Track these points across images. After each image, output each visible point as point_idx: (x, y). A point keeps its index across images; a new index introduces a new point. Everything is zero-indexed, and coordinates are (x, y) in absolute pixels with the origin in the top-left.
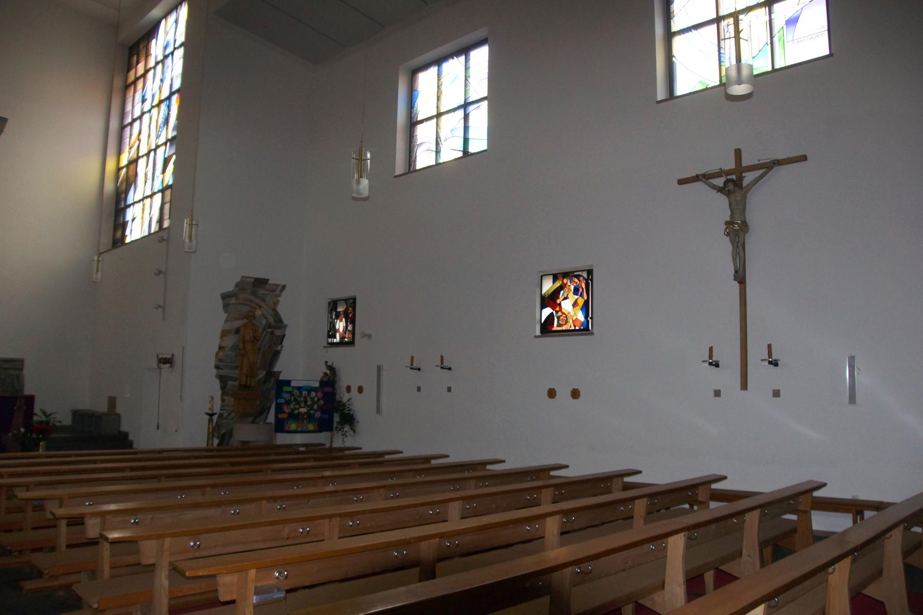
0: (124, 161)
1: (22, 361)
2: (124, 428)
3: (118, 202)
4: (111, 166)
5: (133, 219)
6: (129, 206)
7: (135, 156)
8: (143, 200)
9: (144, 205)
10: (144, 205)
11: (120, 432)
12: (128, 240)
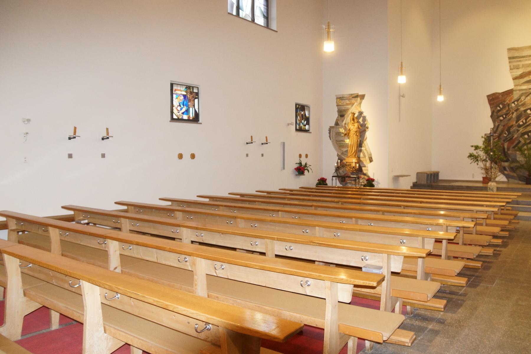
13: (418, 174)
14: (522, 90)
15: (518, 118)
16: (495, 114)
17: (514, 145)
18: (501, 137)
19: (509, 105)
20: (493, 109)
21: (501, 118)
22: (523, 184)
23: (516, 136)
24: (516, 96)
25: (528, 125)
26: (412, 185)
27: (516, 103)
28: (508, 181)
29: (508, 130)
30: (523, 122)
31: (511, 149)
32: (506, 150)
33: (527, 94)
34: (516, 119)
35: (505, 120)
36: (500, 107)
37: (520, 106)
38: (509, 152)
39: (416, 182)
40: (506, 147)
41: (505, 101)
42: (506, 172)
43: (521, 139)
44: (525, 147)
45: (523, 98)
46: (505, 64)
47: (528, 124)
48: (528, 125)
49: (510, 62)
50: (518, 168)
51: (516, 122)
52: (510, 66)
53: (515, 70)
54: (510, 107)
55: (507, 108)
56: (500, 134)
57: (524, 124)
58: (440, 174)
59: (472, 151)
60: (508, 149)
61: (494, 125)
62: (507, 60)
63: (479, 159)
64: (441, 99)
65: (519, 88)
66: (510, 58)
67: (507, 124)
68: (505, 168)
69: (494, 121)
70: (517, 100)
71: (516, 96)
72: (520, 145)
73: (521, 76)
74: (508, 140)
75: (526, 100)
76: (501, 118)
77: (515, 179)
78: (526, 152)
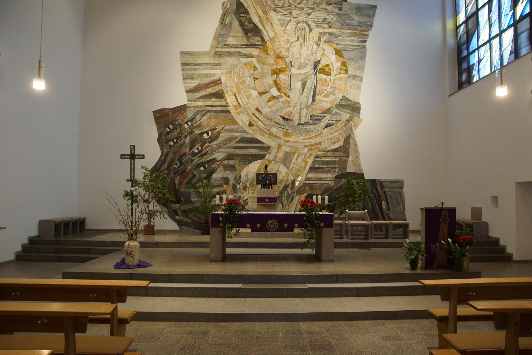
0: (462, 18)
1: (402, 182)
2: (493, 233)
3: (459, 52)
4: (450, 25)
5: (479, 61)
6: (474, 51)
7: (474, 9)
8: (489, 41)
9: (491, 46)
10: (491, 46)
11: (488, 237)
12: (475, 79)
13: (42, 223)
14: (197, 107)
15: (193, 144)
16: (163, 137)
17: (187, 180)
18: (171, 168)
19: (181, 126)
20: (160, 130)
21: (171, 143)
22: (198, 235)
23: (189, 168)
24: (189, 114)
25: (206, 153)
26: (26, 241)
27: (190, 123)
28: (181, 229)
29: (180, 160)
30: (198, 149)
31: (184, 185)
32: (177, 188)
33: (203, 113)
34: (189, 146)
35: (175, 146)
36: (169, 128)
37: (194, 128)
38: (181, 190)
39: (38, 236)
40: (177, 182)
41: (176, 121)
42: (177, 217)
43: (196, 173)
44: (200, 184)
45: (198, 117)
46: (177, 72)
47: (204, 152)
48: (206, 153)
49: (183, 70)
50: (192, 211)
51: (190, 150)
52: (183, 75)
53: (188, 81)
54: (182, 128)
55: (179, 130)
56: (170, 165)
57: (200, 152)
58: (86, 221)
59: (128, 187)
60: (180, 184)
61: (162, 152)
62: (180, 67)
63: (139, 198)
64: (39, 85)
65: (193, 104)
66: (183, 64)
67: (178, 151)
68: (176, 212)
69: (162, 148)
70: (191, 120)
71: (189, 114)
72: (195, 180)
73: (196, 89)
74: (180, 174)
75: (202, 121)
76: (171, 143)
77: (189, 227)
78: (201, 190)
